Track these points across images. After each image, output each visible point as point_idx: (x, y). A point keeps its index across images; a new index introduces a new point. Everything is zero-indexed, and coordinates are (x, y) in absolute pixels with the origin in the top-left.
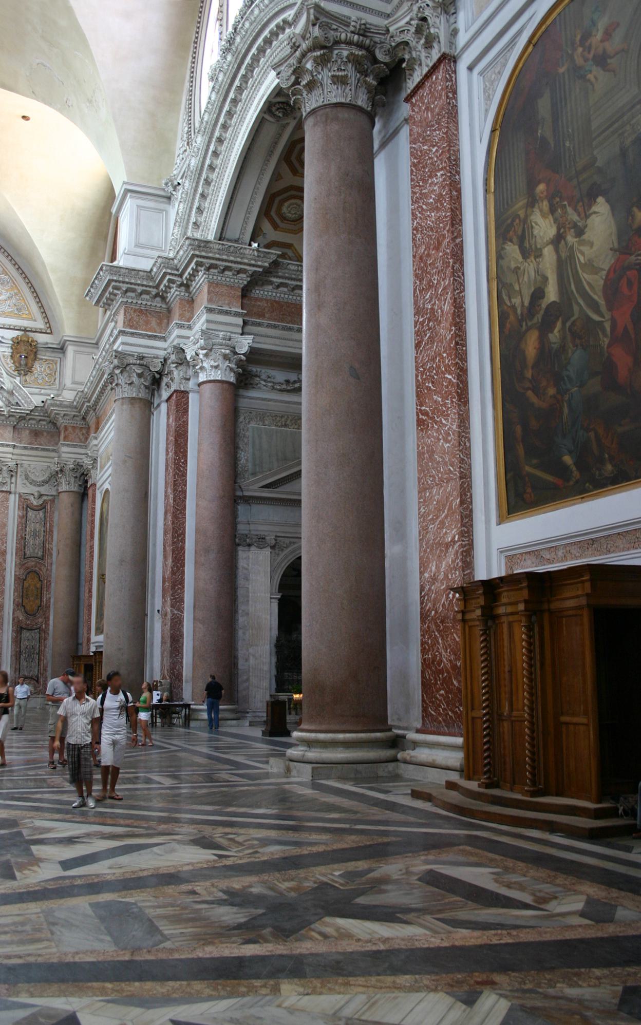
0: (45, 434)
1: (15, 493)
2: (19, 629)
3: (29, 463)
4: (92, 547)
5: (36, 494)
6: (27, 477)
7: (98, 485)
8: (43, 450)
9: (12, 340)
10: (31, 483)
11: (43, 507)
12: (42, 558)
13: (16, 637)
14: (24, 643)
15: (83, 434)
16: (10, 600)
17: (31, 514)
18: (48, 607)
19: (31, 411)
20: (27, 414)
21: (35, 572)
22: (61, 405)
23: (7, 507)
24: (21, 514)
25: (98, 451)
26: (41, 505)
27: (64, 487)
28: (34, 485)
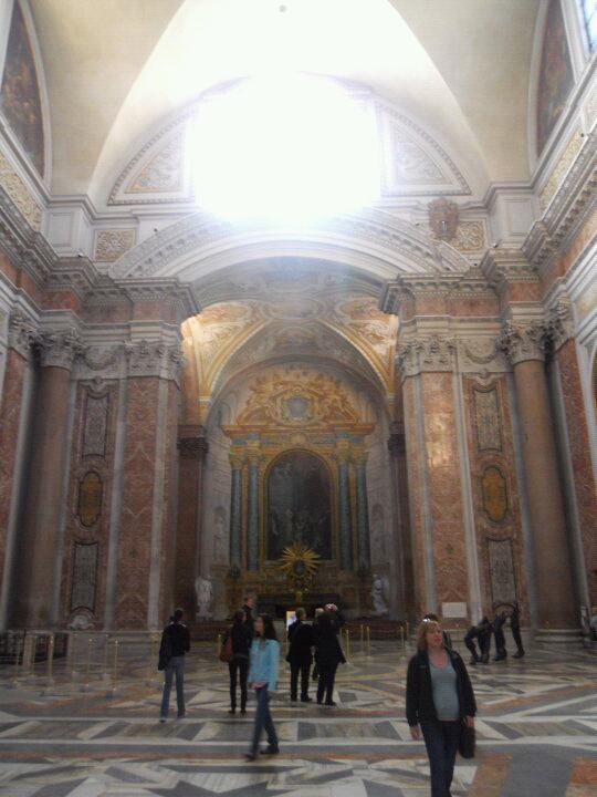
1: (458, 374)
2: (485, 540)
3: (470, 337)
7: (578, 340)
8: (483, 320)
9: (429, 205)
11: (492, 388)
12: (501, 449)
13: (483, 551)
14: (494, 559)
15: (534, 292)
17: (479, 396)
18: (517, 511)
19: (466, 274)
20: (462, 279)
21: (493, 467)
25: (569, 297)
27: (520, 356)
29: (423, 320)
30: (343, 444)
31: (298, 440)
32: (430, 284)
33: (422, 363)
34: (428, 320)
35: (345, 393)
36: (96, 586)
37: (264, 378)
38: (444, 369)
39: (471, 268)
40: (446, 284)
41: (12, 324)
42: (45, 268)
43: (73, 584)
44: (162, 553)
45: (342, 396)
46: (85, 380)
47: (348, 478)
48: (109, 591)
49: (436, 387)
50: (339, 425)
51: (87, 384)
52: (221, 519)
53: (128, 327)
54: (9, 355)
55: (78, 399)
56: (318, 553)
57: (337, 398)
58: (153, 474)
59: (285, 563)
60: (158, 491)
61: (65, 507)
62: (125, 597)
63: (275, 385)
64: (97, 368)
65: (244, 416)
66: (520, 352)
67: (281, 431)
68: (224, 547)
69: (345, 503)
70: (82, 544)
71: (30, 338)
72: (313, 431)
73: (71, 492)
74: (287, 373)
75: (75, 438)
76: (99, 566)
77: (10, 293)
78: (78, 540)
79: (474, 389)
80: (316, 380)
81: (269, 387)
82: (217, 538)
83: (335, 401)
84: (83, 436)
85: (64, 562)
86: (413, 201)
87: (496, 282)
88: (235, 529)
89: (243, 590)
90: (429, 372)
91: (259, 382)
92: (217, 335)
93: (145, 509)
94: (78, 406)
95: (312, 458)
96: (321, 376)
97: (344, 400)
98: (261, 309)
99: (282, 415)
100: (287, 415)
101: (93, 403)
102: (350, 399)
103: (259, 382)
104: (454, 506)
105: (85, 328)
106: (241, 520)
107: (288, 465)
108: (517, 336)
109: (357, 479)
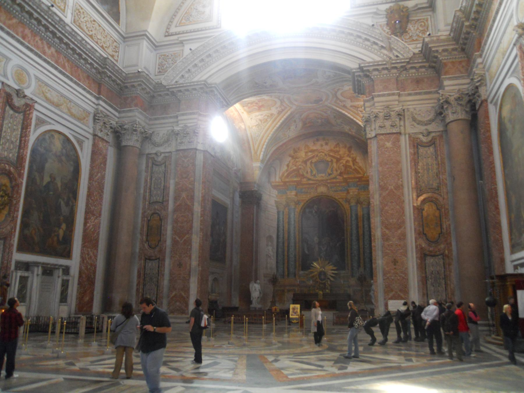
0: (426, 80)
1: (405, 135)
3: (414, 106)
4: (492, 163)
5: (425, 132)
6: (414, 119)
7: (489, 100)
8: (426, 93)
10: (418, 124)
11: (432, 143)
15: (463, 67)
16: (411, 229)
19: (410, 59)
22: (439, 40)
23: (399, 147)
24: (412, 151)
26: (430, 141)
27: (451, 117)
28: (422, 125)
29: (379, 96)
30: (353, 191)
31: (322, 189)
32: (383, 69)
33: (377, 128)
34: (383, 95)
35: (354, 156)
36: (158, 287)
37: (299, 149)
38: (394, 131)
39: (414, 54)
40: (396, 68)
41: (95, 119)
42: (119, 81)
43: (144, 285)
44: (199, 265)
45: (353, 158)
46: (151, 154)
47: (357, 215)
48: (165, 290)
49: (389, 145)
50: (349, 178)
51: (153, 156)
52: (270, 244)
53: (177, 117)
54: (94, 139)
55: (147, 167)
56: (335, 266)
57: (350, 159)
58: (192, 215)
59: (312, 272)
60: (196, 224)
61: (139, 236)
62: (174, 294)
63: (306, 153)
64: (159, 146)
65: (286, 174)
66: (450, 114)
67: (312, 184)
68: (272, 262)
69: (354, 232)
70: (150, 260)
71: (111, 128)
72: (333, 183)
73: (143, 226)
74: (314, 143)
75: (145, 191)
76: (160, 273)
77: (93, 99)
78: (147, 257)
79: (418, 144)
80: (334, 148)
81: (302, 154)
82: (268, 256)
83: (347, 161)
84: (150, 189)
85: (139, 272)
86: (373, 9)
87: (435, 62)
88: (280, 250)
89: (286, 291)
90: (383, 134)
91: (295, 151)
92: (260, 120)
93: (187, 236)
94: (146, 172)
95: (331, 201)
96: (337, 145)
97: (354, 160)
98: (285, 100)
99: (311, 172)
100: (314, 173)
101: (156, 169)
102: (358, 159)
103: (295, 151)
104: (399, 232)
105: (150, 119)
106: (283, 243)
107: (315, 206)
108: (447, 102)
109: (363, 215)
